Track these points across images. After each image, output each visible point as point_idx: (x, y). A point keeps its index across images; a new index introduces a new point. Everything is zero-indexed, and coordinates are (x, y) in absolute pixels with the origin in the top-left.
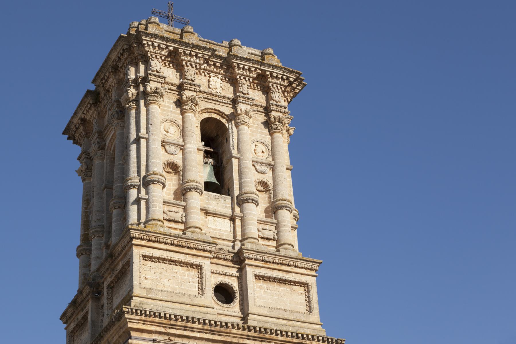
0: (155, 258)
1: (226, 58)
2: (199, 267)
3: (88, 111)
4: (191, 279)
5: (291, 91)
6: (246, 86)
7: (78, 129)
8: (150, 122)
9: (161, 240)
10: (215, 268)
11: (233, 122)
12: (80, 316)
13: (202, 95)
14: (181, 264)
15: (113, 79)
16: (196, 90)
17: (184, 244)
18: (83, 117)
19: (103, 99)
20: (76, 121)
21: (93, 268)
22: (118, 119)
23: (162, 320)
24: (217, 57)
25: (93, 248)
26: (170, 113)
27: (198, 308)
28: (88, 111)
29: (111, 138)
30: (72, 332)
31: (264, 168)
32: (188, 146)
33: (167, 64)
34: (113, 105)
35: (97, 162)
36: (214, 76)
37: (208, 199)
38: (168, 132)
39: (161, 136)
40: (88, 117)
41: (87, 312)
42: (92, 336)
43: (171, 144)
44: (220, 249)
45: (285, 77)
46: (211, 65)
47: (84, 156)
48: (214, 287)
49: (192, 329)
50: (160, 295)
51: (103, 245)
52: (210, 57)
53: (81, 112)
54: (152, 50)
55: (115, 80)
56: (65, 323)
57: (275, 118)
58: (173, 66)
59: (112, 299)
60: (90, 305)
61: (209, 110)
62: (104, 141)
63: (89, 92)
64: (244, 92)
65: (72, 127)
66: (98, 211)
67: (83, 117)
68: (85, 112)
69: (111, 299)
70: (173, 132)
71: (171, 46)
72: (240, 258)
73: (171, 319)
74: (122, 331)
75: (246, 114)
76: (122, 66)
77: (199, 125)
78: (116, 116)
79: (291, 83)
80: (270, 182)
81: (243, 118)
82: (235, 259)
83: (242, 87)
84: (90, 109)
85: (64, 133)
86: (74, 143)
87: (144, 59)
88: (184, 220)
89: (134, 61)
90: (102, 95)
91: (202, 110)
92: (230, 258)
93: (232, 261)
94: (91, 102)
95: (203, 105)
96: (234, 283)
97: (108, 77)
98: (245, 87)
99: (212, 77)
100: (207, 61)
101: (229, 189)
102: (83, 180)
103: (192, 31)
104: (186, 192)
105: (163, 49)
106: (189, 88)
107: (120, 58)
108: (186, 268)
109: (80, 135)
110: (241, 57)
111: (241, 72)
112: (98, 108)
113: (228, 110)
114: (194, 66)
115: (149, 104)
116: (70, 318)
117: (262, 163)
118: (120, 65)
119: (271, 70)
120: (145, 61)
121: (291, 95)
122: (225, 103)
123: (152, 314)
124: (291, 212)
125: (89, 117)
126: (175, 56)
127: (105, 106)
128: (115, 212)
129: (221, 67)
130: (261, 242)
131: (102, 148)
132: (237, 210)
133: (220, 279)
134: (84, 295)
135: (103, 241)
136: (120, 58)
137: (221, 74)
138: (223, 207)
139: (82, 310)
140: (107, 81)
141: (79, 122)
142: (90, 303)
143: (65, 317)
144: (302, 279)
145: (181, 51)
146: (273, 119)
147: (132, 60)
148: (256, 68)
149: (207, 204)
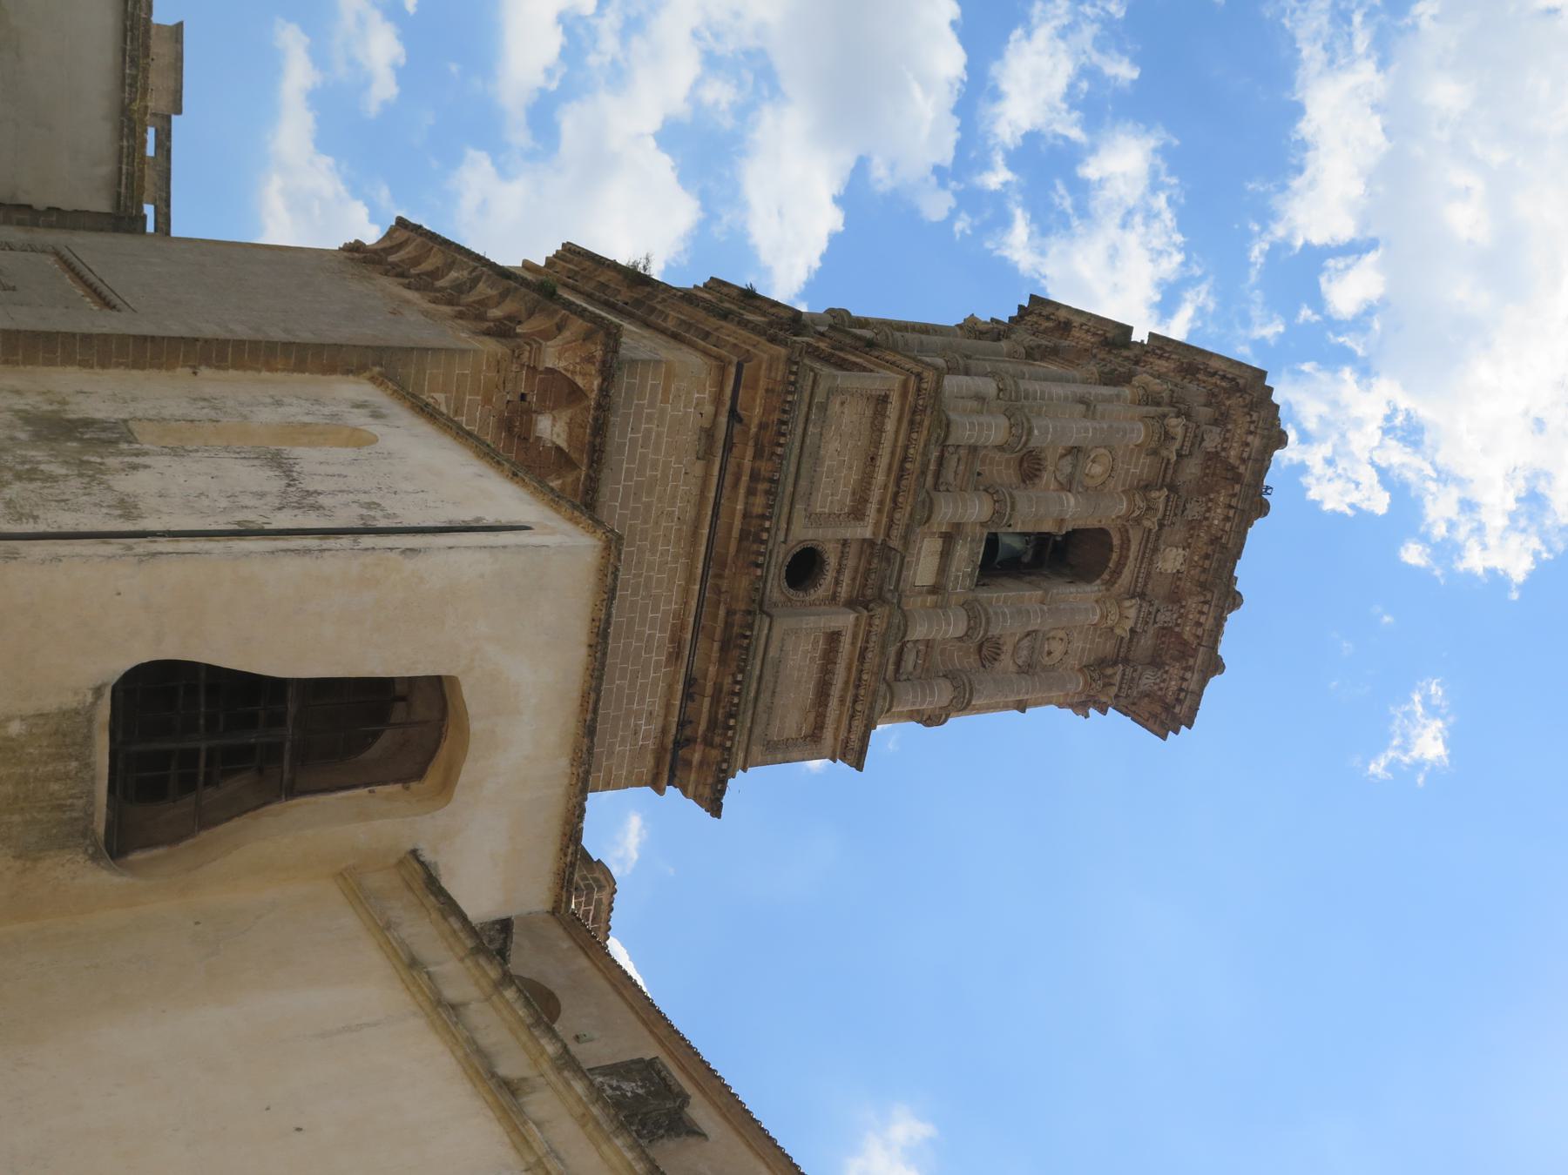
2: (857, 514)
3: (1088, 331)
4: (838, 498)
6: (1168, 619)
15: (1166, 367)
19: (1117, 356)
20: (1062, 314)
22: (1102, 373)
26: (1126, 467)
28: (1088, 331)
36: (1184, 556)
40: (1076, 333)
43: (1074, 466)
48: (820, 548)
55: (1165, 370)
66: (921, 343)
67: (1075, 324)
71: (1246, 469)
72: (870, 601)
76: (1199, 380)
83: (1168, 611)
84: (1094, 334)
90: (1125, 353)
91: (1127, 531)
94: (1108, 335)
97: (1168, 358)
101: (984, 585)
102: (959, 326)
107: (1215, 374)
112: (1097, 348)
119: (1196, 667)
120: (1216, 419)
122: (1138, 577)
125: (1078, 335)
126: (1227, 479)
133: (832, 560)
136: (1215, 374)
140: (1161, 357)
141: (1062, 320)
144: (829, 730)
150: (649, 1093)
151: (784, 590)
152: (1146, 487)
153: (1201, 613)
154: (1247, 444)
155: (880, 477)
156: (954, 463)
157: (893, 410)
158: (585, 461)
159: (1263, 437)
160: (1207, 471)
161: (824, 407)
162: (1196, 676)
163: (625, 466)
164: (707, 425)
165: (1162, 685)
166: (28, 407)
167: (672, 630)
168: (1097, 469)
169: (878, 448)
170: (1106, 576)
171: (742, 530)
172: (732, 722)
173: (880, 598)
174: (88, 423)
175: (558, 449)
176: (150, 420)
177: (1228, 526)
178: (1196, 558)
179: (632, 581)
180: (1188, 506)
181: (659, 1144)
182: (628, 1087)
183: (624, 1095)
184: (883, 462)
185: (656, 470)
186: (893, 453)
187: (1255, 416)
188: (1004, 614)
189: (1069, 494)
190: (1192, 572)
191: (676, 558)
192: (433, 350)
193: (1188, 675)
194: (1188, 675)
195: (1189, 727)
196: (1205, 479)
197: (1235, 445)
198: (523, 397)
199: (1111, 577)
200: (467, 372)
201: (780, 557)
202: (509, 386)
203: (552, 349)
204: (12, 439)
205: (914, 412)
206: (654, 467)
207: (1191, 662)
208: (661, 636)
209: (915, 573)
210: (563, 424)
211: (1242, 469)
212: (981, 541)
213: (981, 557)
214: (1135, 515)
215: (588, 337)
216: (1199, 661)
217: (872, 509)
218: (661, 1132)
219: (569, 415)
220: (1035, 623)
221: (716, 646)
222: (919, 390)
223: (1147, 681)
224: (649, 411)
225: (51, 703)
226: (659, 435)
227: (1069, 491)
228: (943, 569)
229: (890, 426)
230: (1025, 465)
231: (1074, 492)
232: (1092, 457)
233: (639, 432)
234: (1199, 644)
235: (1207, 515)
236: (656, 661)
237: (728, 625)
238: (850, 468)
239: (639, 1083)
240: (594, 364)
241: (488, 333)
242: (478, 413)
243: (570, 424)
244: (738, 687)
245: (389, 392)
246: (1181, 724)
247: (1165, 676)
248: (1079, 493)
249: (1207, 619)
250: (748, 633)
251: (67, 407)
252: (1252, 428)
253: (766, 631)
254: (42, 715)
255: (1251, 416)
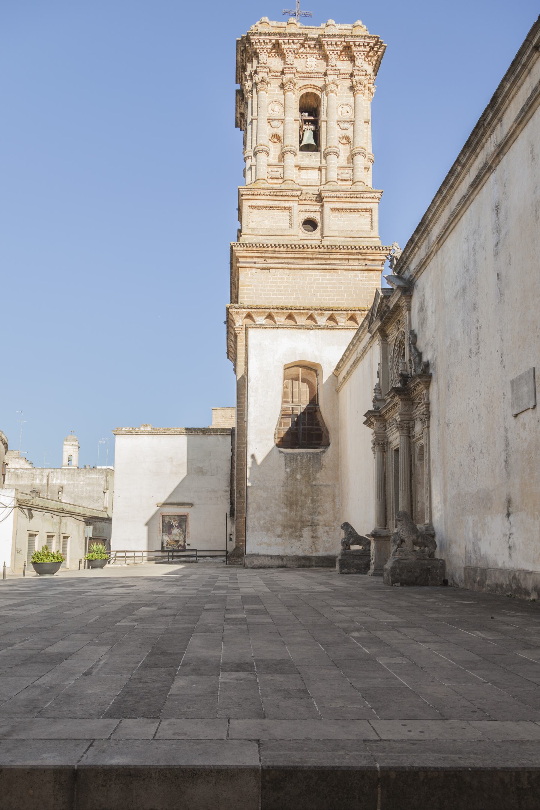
0: (258, 207)
1: (317, 39)
5: (374, 55)
6: (335, 59)
8: (259, 106)
9: (262, 193)
10: (303, 208)
11: (324, 92)
13: (297, 75)
14: (278, 208)
17: (278, 194)
23: (258, 249)
24: (311, 39)
27: (287, 238)
31: (347, 125)
32: (287, 119)
33: (273, 55)
37: (303, 158)
39: (268, 115)
44: (307, 193)
45: (366, 44)
46: (307, 48)
49: (279, 252)
52: (305, 41)
54: (259, 47)
57: (356, 82)
58: (278, 55)
61: (306, 87)
64: (332, 65)
70: (277, 110)
73: (264, 247)
75: (333, 83)
79: (372, 48)
80: (351, 136)
81: (333, 87)
82: (318, 199)
88: (282, 176)
92: (315, 199)
93: (316, 200)
95: (301, 83)
96: (317, 217)
98: (333, 59)
99: (309, 58)
100: (302, 45)
103: (295, 21)
104: (284, 155)
105: (267, 43)
108: (281, 211)
110: (328, 35)
111: (330, 47)
113: (320, 83)
114: (292, 52)
115: (259, 91)
117: (345, 121)
121: (375, 58)
123: (251, 245)
124: (365, 157)
129: (315, 47)
130: (340, 182)
132: (324, 161)
137: (316, 53)
138: (313, 162)
145: (281, 41)
146: (355, 83)
147: (249, 58)
148: (342, 42)
149: (302, 161)
207: (351, 43)
217: (287, 204)
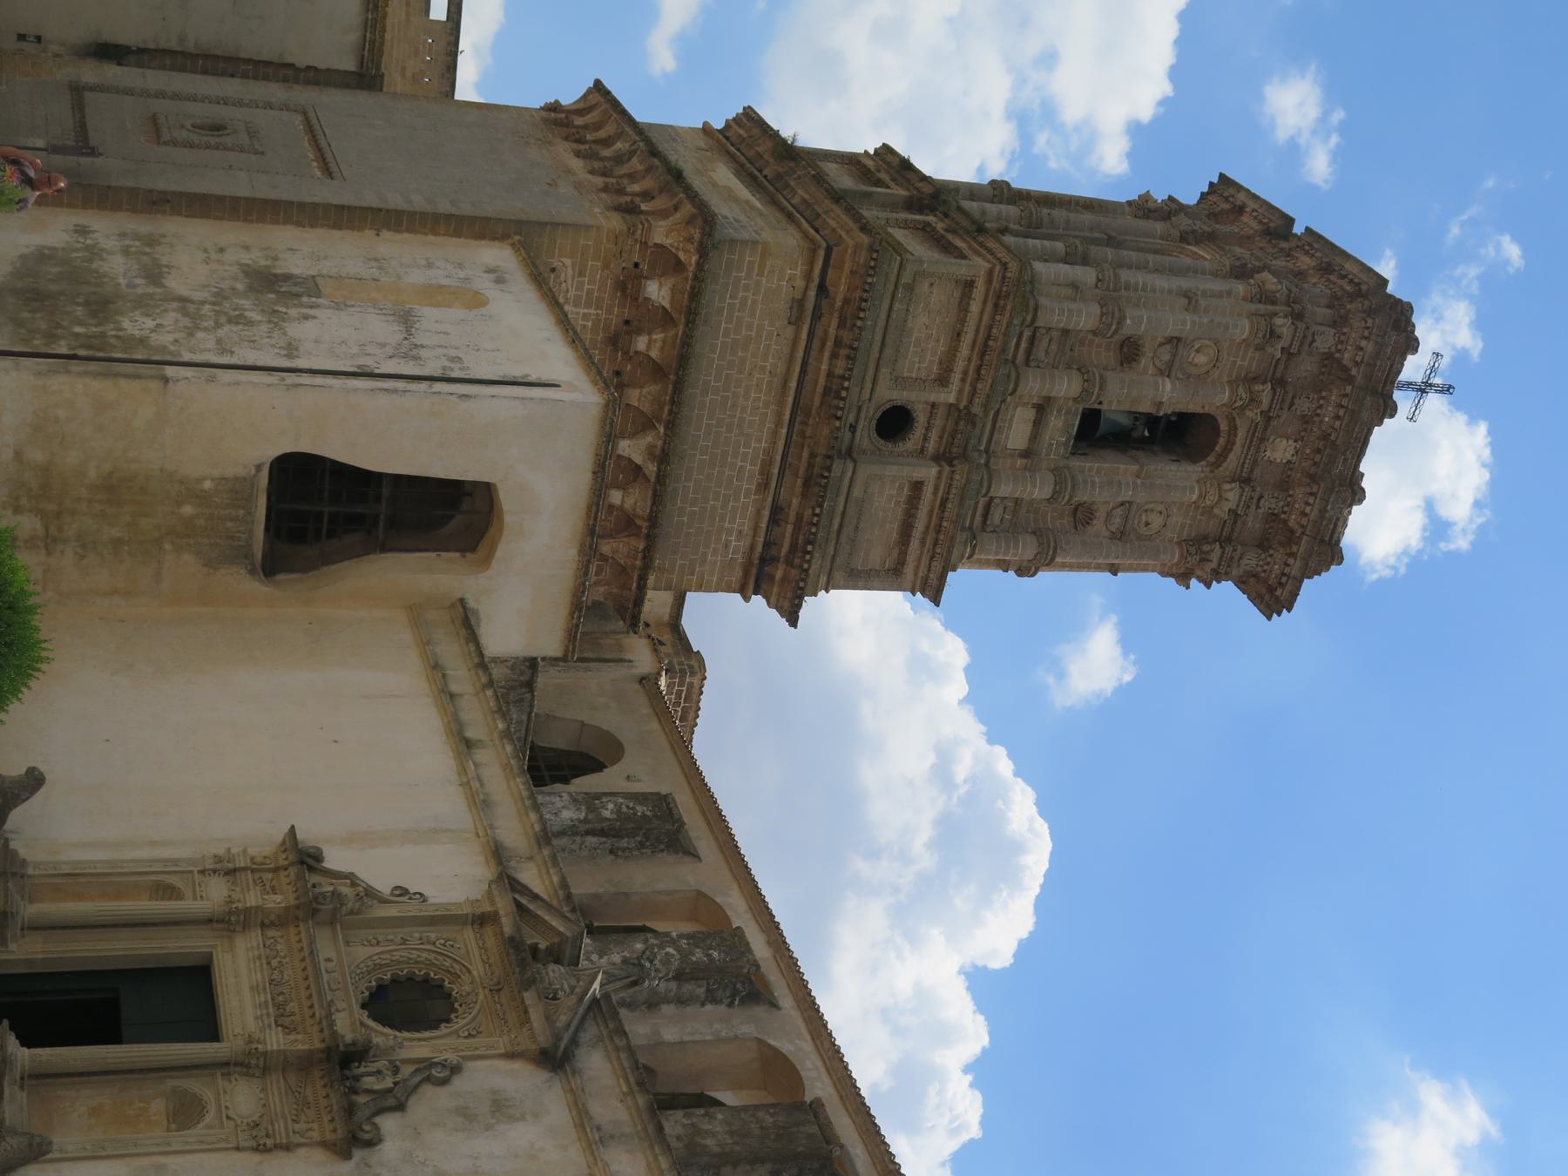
2: (943, 380)
3: (1255, 218)
6: (1273, 506)
7: (1227, 199)
12: (883, 176)
15: (1308, 265)
16: (1272, 410)
18: (1247, 210)
19: (1275, 246)
21: (966, 204)
22: (1232, 267)
25: (1003, 207)
26: (1232, 359)
27: (871, 373)
28: (1255, 218)
29: (1200, 255)
30: (859, 162)
34: (1258, 259)
35: (1159, 227)
36: (1296, 447)
38: (1198, 351)
40: (1245, 219)
41: (888, 187)
42: (845, 191)
43: (1174, 355)
47: (1173, 206)
48: (909, 407)
50: (900, 307)
51: (1004, 223)
53: (1256, 206)
55: (1306, 267)
56: (876, 150)
59: (904, 228)
60: (901, 192)
62: (1197, 243)
63: (1290, 221)
64: (1262, 501)
65: (1232, 191)
67: (1247, 210)
68: (1255, 214)
69: (905, 225)
71: (1358, 372)
72: (955, 458)
74: (843, 234)
76: (1331, 281)
77: (1206, 410)
78: (1238, 263)
83: (1273, 498)
85: (1222, 176)
86: (1202, 194)
87: (1339, 320)
89: (1336, 303)
90: (1284, 245)
91: (1234, 419)
94: (1272, 225)
97: (1313, 256)
99: (1295, 444)
104: (1083, 374)
106: (1276, 397)
107: (1345, 277)
109: (1215, 203)
112: (1260, 236)
116: (883, 160)
118: (1332, 277)
120: (1335, 322)
122: (1244, 463)
125: (1246, 220)
127: (1261, 248)
128: (1059, 246)
131: (1184, 238)
133: (921, 419)
134: (919, 185)
135: (1012, 226)
136: (1345, 277)
139: (894, 180)
140: (1307, 253)
142: (902, 192)
143: (886, 151)
150: (655, 816)
151: (874, 440)
152: (1251, 380)
153: (1307, 504)
154: (1362, 349)
155: (964, 351)
156: (1045, 343)
157: (978, 292)
158: (683, 320)
159: (1377, 343)
160: (1324, 370)
161: (910, 288)
162: (1298, 563)
163: (723, 325)
164: (798, 296)
165: (1266, 567)
166: (250, 262)
167: (761, 465)
168: (1201, 359)
169: (963, 325)
170: (1211, 458)
171: (825, 387)
172: (809, 548)
173: (964, 456)
174: (287, 277)
175: (664, 308)
176: (331, 277)
177: (1337, 424)
178: (1308, 451)
179: (726, 420)
180: (1297, 401)
181: (660, 856)
182: (640, 809)
183: (635, 814)
184: (967, 339)
185: (751, 331)
186: (977, 331)
187: (1370, 322)
188: (1093, 483)
189: (1167, 380)
190: (1303, 464)
191: (767, 406)
192: (565, 225)
193: (1291, 561)
194: (1291, 561)
195: (1289, 611)
196: (1321, 377)
197: (1349, 348)
198: (636, 265)
199: (1217, 459)
200: (590, 243)
201: (871, 414)
202: (624, 255)
203: (662, 229)
204: (233, 289)
205: (999, 297)
206: (750, 327)
207: (1294, 549)
208: (752, 469)
209: (1007, 437)
210: (667, 289)
211: (1354, 372)
212: (1077, 415)
213: (1075, 429)
214: (1237, 404)
215: (690, 221)
216: (1302, 549)
217: (956, 378)
218: (662, 847)
219: (670, 285)
220: (1126, 495)
221: (799, 482)
222: (1004, 277)
223: (1249, 562)
224: (746, 282)
225: (230, 472)
226: (754, 302)
227: (1168, 376)
228: (1035, 436)
229: (975, 307)
230: (1125, 349)
231: (1173, 378)
232: (1196, 347)
233: (736, 299)
234: (1303, 533)
235: (1319, 411)
236: (747, 489)
237: (810, 465)
238: (938, 340)
239: (650, 808)
240: (693, 243)
241: (618, 209)
242: (598, 277)
243: (672, 290)
244: (816, 519)
245: (520, 259)
246: (1284, 607)
247: (1269, 559)
248: (1178, 379)
249: (1312, 510)
250: (826, 474)
251: (277, 263)
252: (1366, 333)
253: (850, 474)
254: (224, 478)
255: (1366, 322)
